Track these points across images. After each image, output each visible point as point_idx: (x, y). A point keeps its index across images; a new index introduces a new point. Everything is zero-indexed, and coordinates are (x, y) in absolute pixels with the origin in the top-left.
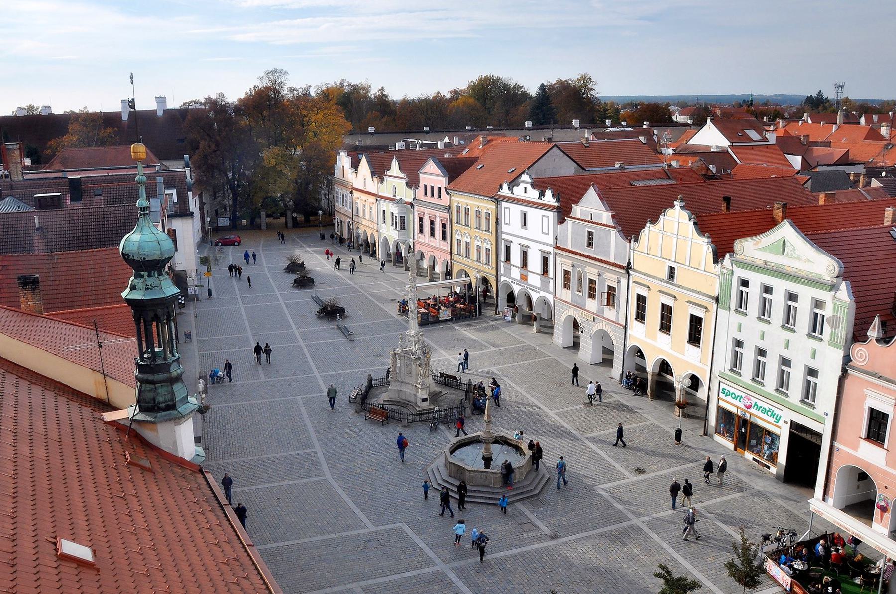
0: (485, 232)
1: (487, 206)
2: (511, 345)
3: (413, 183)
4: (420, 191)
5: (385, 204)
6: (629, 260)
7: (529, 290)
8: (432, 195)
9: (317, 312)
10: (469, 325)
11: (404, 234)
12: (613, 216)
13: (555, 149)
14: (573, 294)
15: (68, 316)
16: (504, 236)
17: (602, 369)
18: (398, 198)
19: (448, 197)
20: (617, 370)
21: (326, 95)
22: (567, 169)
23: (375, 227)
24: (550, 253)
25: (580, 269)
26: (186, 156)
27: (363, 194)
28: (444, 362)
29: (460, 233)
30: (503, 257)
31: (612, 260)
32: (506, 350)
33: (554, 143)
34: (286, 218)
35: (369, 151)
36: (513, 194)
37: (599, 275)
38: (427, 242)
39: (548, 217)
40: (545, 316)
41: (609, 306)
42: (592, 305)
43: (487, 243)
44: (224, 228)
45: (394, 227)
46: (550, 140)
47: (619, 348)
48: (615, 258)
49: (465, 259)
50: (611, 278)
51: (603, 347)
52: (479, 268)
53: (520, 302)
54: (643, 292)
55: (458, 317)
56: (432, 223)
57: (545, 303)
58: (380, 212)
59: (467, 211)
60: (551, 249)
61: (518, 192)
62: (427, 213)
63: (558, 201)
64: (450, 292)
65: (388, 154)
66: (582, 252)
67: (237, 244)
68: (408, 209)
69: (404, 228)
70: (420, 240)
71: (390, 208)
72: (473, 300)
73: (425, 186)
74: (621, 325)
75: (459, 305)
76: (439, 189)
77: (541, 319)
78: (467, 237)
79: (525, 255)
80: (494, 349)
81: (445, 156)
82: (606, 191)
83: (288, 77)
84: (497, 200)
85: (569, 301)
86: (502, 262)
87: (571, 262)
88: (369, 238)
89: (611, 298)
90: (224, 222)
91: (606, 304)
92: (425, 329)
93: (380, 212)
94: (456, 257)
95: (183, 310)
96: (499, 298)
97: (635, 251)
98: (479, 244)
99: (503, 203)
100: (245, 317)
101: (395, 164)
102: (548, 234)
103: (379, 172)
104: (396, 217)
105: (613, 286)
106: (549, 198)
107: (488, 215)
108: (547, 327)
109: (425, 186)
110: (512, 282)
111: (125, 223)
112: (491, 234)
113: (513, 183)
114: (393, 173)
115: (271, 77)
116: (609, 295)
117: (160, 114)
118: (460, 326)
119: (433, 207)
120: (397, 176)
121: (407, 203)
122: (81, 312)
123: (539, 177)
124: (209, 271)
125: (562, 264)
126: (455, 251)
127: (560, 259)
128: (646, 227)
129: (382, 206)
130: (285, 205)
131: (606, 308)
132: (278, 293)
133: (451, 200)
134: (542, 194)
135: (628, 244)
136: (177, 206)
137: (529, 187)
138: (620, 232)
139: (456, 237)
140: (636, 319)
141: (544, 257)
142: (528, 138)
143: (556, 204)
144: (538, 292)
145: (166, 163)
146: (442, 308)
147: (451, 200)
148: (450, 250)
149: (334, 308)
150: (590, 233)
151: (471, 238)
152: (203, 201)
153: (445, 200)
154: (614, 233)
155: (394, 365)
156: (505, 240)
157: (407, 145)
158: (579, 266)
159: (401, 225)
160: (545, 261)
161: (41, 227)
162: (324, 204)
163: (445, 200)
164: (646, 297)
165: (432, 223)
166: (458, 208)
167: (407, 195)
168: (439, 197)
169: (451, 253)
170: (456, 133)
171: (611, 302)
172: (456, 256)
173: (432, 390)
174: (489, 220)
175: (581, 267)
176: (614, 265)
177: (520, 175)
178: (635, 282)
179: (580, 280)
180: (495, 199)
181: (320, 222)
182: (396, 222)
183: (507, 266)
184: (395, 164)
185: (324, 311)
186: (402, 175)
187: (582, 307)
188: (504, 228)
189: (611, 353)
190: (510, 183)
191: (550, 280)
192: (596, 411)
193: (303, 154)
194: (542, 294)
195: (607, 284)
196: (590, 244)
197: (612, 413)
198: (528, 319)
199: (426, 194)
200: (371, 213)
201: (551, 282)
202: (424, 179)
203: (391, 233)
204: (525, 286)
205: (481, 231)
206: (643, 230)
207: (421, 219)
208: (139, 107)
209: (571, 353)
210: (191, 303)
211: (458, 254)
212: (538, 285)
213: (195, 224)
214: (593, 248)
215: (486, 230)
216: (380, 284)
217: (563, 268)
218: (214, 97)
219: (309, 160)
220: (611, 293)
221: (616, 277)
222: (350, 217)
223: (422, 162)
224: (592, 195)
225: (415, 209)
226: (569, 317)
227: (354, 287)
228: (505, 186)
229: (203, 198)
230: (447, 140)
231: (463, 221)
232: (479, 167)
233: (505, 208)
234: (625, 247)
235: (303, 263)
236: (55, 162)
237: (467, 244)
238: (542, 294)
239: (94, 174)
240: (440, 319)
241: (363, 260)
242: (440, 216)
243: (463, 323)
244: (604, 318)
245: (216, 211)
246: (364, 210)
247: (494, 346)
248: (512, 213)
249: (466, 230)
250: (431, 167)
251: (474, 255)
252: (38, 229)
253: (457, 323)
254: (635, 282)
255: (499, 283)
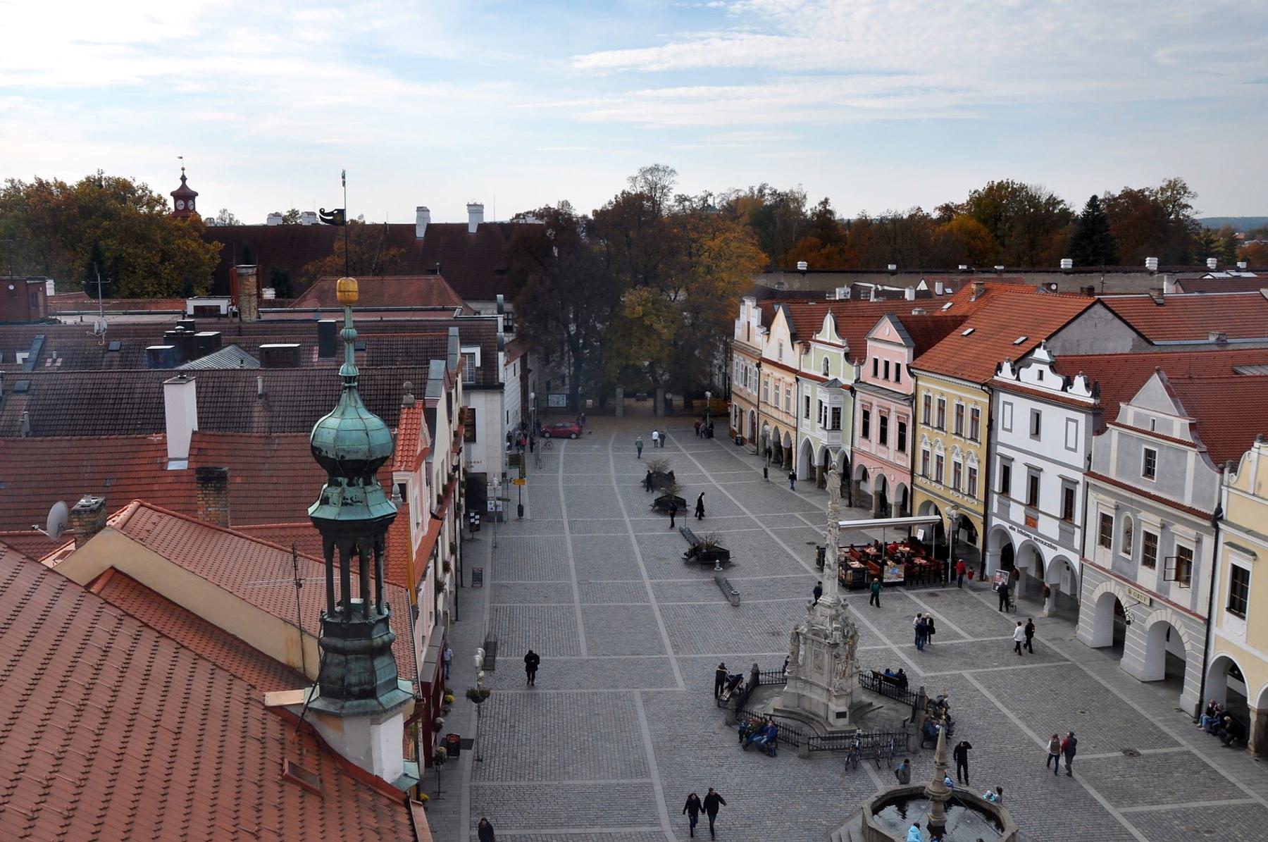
0: (969, 442)
1: (975, 399)
2: (1001, 635)
3: (855, 355)
4: (868, 367)
5: (810, 386)
6: (1220, 504)
7: (1039, 544)
8: (887, 376)
9: (685, 554)
10: (932, 595)
11: (838, 437)
12: (1192, 427)
13: (1098, 307)
14: (1116, 556)
15: (265, 533)
16: (1000, 449)
17: (1162, 693)
18: (831, 377)
19: (912, 381)
20: (1190, 696)
21: (734, 209)
22: (1120, 341)
23: (793, 422)
24: (1077, 482)
25: (1128, 514)
26: (500, 297)
27: (786, 372)
28: (884, 653)
29: (928, 440)
30: (997, 485)
31: (1187, 502)
32: (992, 642)
33: (1097, 297)
34: (655, 403)
35: (791, 301)
36: (1019, 380)
37: (1163, 527)
38: (874, 452)
39: (1076, 421)
40: (1066, 589)
41: (1178, 583)
42: (1148, 578)
43: (972, 460)
44: (557, 411)
45: (822, 425)
46: (1090, 292)
47: (1196, 658)
48: (1195, 498)
49: (934, 484)
50: (1183, 535)
51: (1168, 654)
52: (956, 500)
53: (1019, 563)
54: (1244, 563)
55: (914, 579)
56: (884, 421)
57: (1068, 568)
58: (802, 399)
59: (942, 404)
60: (1079, 477)
61: (1028, 377)
62: (877, 404)
63: (1094, 396)
64: (907, 536)
65: (825, 306)
66: (1134, 485)
67: (574, 436)
68: (845, 396)
69: (839, 427)
70: (863, 448)
71: (818, 394)
72: (942, 551)
73: (876, 361)
74: (1201, 617)
75: (918, 561)
76: (898, 366)
77: (1058, 593)
78: (940, 448)
79: (1034, 484)
80: (971, 639)
81: (913, 313)
82: (1181, 381)
83: (675, 178)
84: (992, 389)
85: (1109, 567)
86: (996, 493)
87: (1114, 501)
88: (782, 440)
89: (1184, 568)
90: (558, 400)
91: (1173, 578)
92: (854, 595)
93: (802, 399)
94: (920, 480)
95: (477, 536)
96: (988, 554)
97: (1230, 490)
98: (959, 460)
99: (1001, 394)
100: (570, 554)
101: (829, 322)
102: (1075, 450)
103: (802, 335)
104: (826, 408)
105: (1190, 548)
106: (1079, 391)
107: (975, 412)
108: (1068, 609)
109: (876, 361)
110: (1010, 528)
111: (390, 395)
112: (978, 445)
113: (1020, 362)
114: (825, 337)
115: (650, 177)
116: (1179, 561)
117: (473, 229)
118: (918, 595)
119: (886, 395)
120: (832, 342)
121: (845, 387)
122: (298, 527)
123: (1069, 353)
124: (522, 475)
125: (1095, 505)
126: (919, 470)
127: (1095, 495)
128: (1253, 449)
129: (805, 389)
130: (655, 380)
131: (1174, 586)
132: (627, 519)
133: (916, 385)
134: (1068, 383)
135: (1218, 476)
136: (481, 372)
137: (1046, 369)
138: (1204, 454)
139: (922, 446)
140: (1229, 609)
141: (1067, 489)
142: (1054, 287)
143: (1092, 401)
144: (1055, 548)
145: (475, 306)
146: (889, 563)
147: (916, 385)
148: (910, 467)
149: (712, 550)
150: (1150, 454)
151: (946, 449)
152: (528, 367)
153: (907, 384)
154: (1192, 455)
155: (795, 653)
156: (1003, 457)
157: (856, 292)
158: (1127, 509)
159: (833, 423)
160: (1069, 496)
161: (266, 394)
162: (718, 381)
163: (907, 384)
164: (1248, 572)
165: (884, 421)
166: (928, 398)
167: (845, 373)
168: (898, 379)
169: (912, 472)
170: (940, 276)
171: (1184, 576)
172: (920, 478)
173: (855, 701)
174: (977, 421)
175: (1132, 511)
176: (1190, 511)
177: (1033, 350)
178: (1230, 544)
179: (1128, 532)
180: (988, 387)
181: (708, 410)
182: (825, 417)
183: (1004, 501)
184: (829, 322)
185: (695, 554)
186: (840, 342)
187: (1130, 581)
188: (1001, 436)
189: (1182, 663)
190: (1016, 362)
191: (1076, 529)
192: (1145, 766)
193: (687, 300)
194: (1062, 551)
195: (1176, 543)
196: (1149, 472)
197: (1176, 775)
198: (1038, 591)
199: (876, 373)
200: (788, 400)
201: (1078, 532)
202: (874, 350)
203: (815, 434)
204: (1033, 536)
205: (963, 440)
206: (1247, 453)
207: (866, 415)
208: (435, 220)
209: (1107, 658)
210: (491, 525)
211: (924, 476)
212: (1055, 535)
213: (506, 401)
214: (1153, 479)
215: (971, 439)
216: (792, 517)
217: (1100, 510)
218: (554, 205)
219: (695, 310)
220: (1184, 554)
221: (1192, 533)
222: (754, 405)
223: (874, 321)
224: (1155, 385)
225: (858, 395)
226: (1107, 595)
227: (749, 518)
228: (1007, 367)
229: (528, 361)
230: (923, 286)
231: (934, 421)
232: (965, 333)
233: (1005, 403)
234: (1213, 480)
235: (671, 473)
236: (308, 296)
237: (940, 458)
238: (1062, 551)
239: (362, 317)
240: (884, 581)
241: (769, 475)
242: (897, 410)
243: (923, 591)
244: (1169, 602)
245: (548, 383)
246: (777, 395)
247: (971, 634)
248: (1015, 413)
249: (940, 436)
250: (887, 328)
251: (948, 478)
252: (260, 396)
253: (914, 589)
254: (1230, 544)
255: (989, 528)
